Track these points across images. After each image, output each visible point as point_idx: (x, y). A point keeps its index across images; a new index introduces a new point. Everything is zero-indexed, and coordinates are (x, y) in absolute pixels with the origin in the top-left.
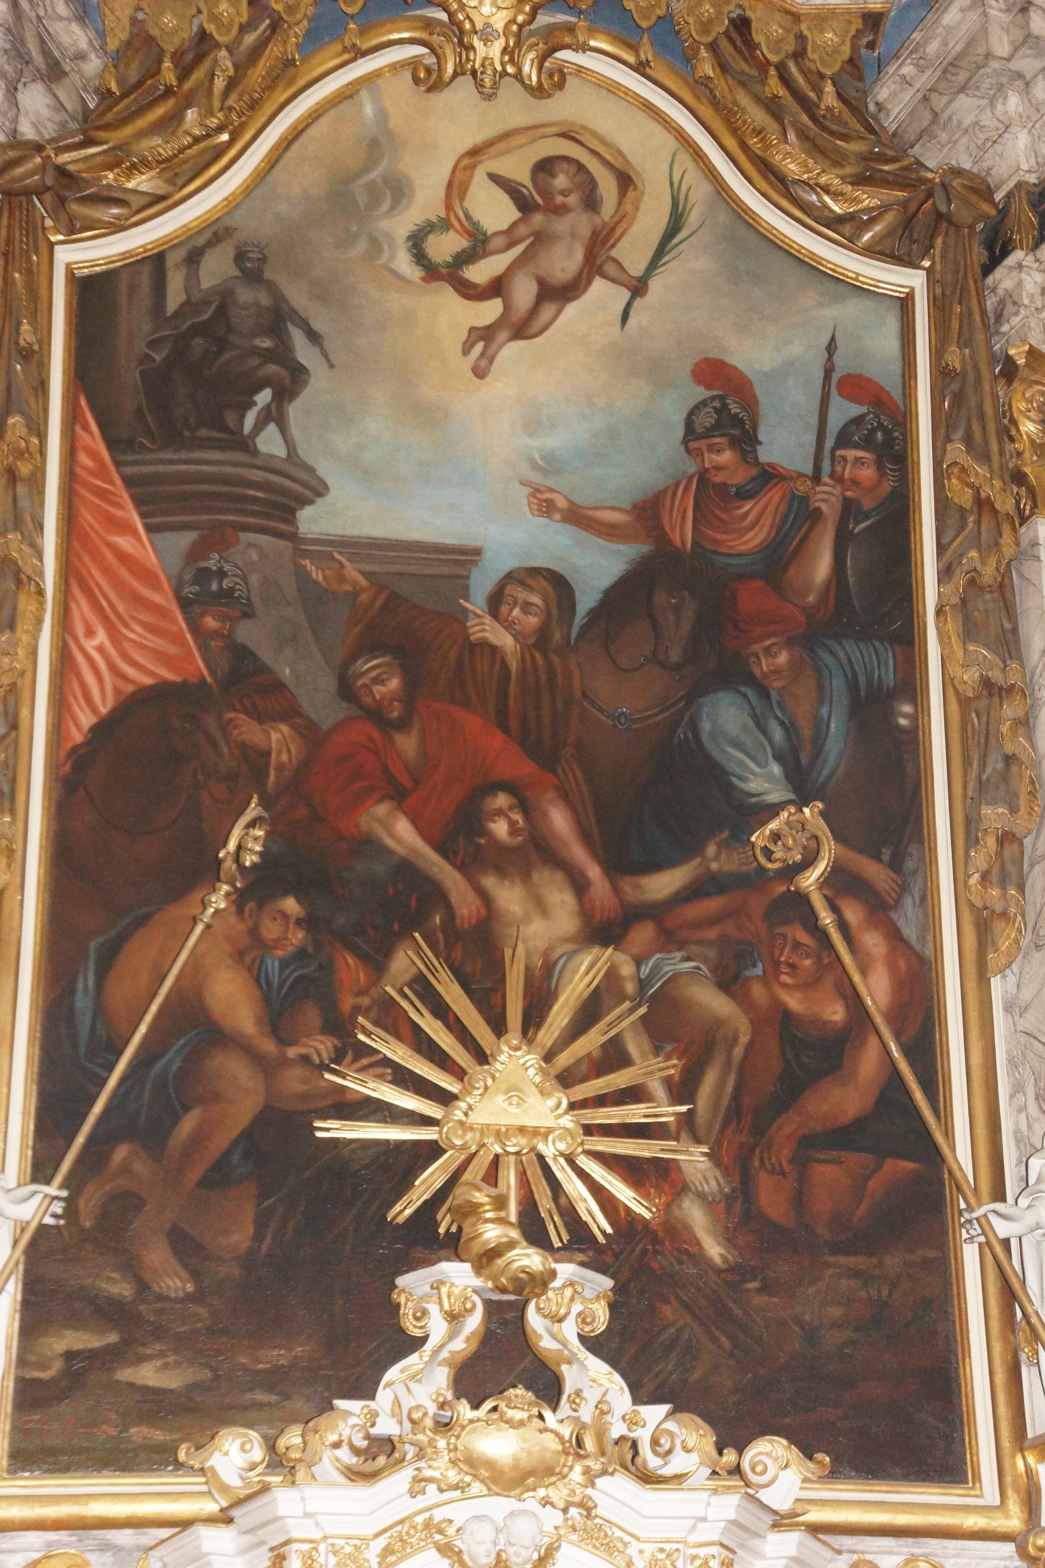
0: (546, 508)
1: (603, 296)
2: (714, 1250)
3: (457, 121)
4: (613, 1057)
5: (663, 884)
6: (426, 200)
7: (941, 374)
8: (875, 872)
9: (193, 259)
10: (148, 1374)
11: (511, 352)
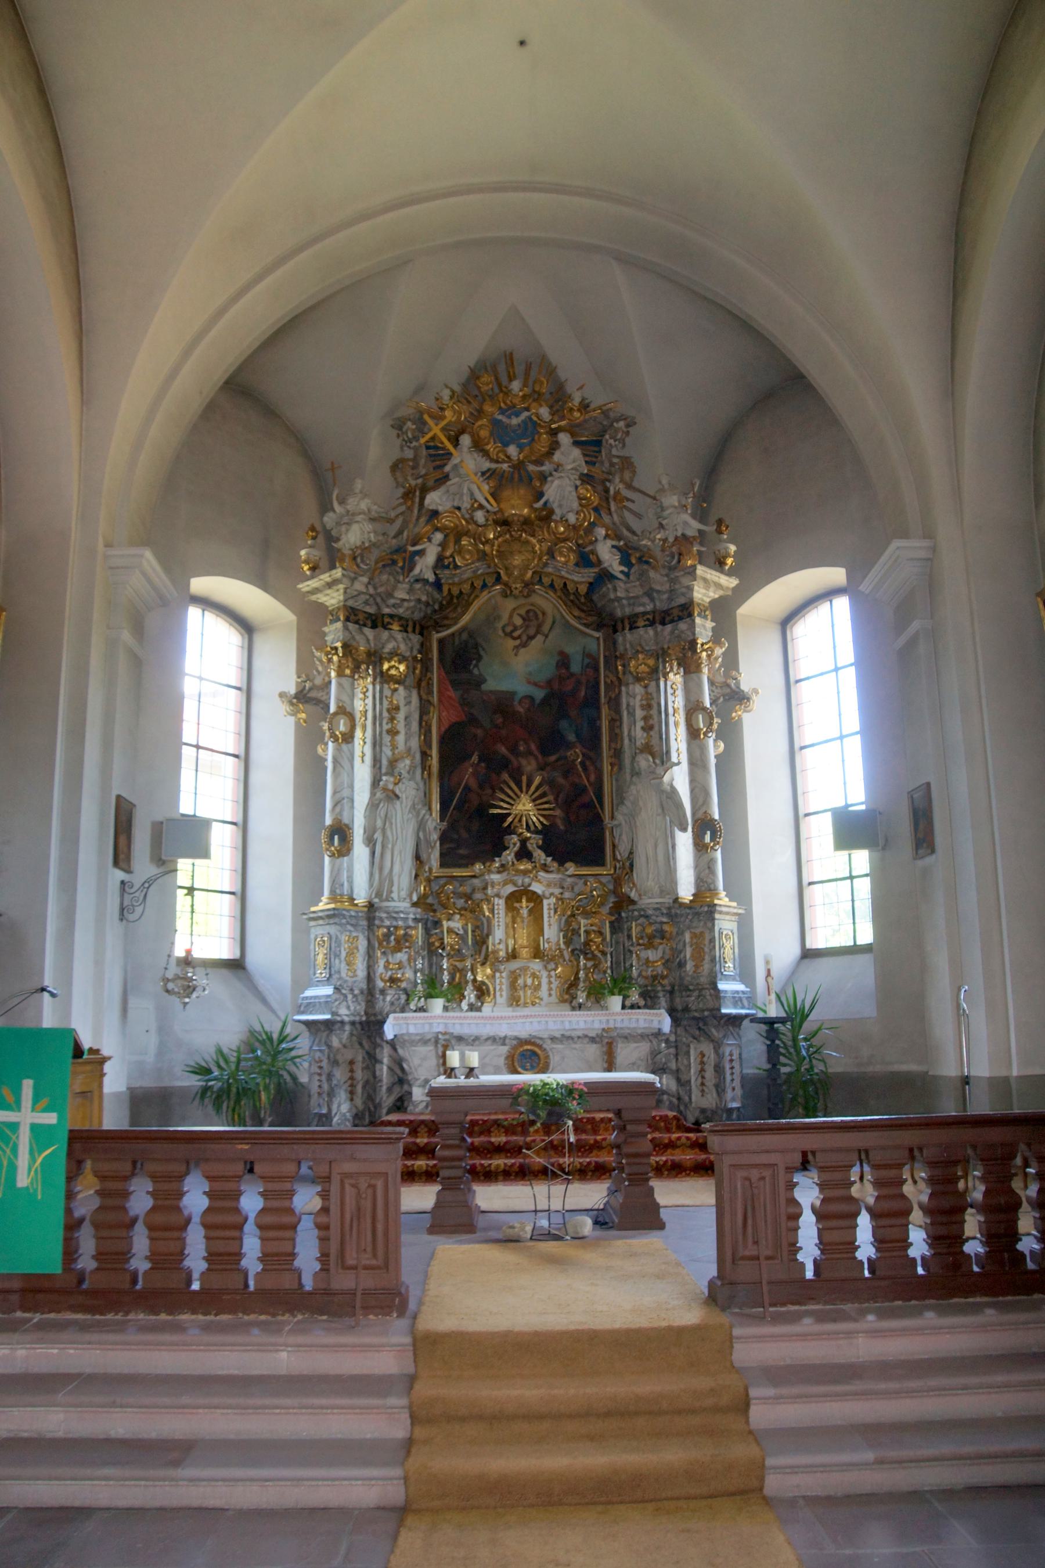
0: (529, 682)
1: (540, 638)
2: (562, 827)
4: (544, 795)
5: (553, 758)
6: (505, 619)
7: (605, 657)
8: (592, 754)
9: (460, 634)
10: (461, 851)
11: (522, 651)
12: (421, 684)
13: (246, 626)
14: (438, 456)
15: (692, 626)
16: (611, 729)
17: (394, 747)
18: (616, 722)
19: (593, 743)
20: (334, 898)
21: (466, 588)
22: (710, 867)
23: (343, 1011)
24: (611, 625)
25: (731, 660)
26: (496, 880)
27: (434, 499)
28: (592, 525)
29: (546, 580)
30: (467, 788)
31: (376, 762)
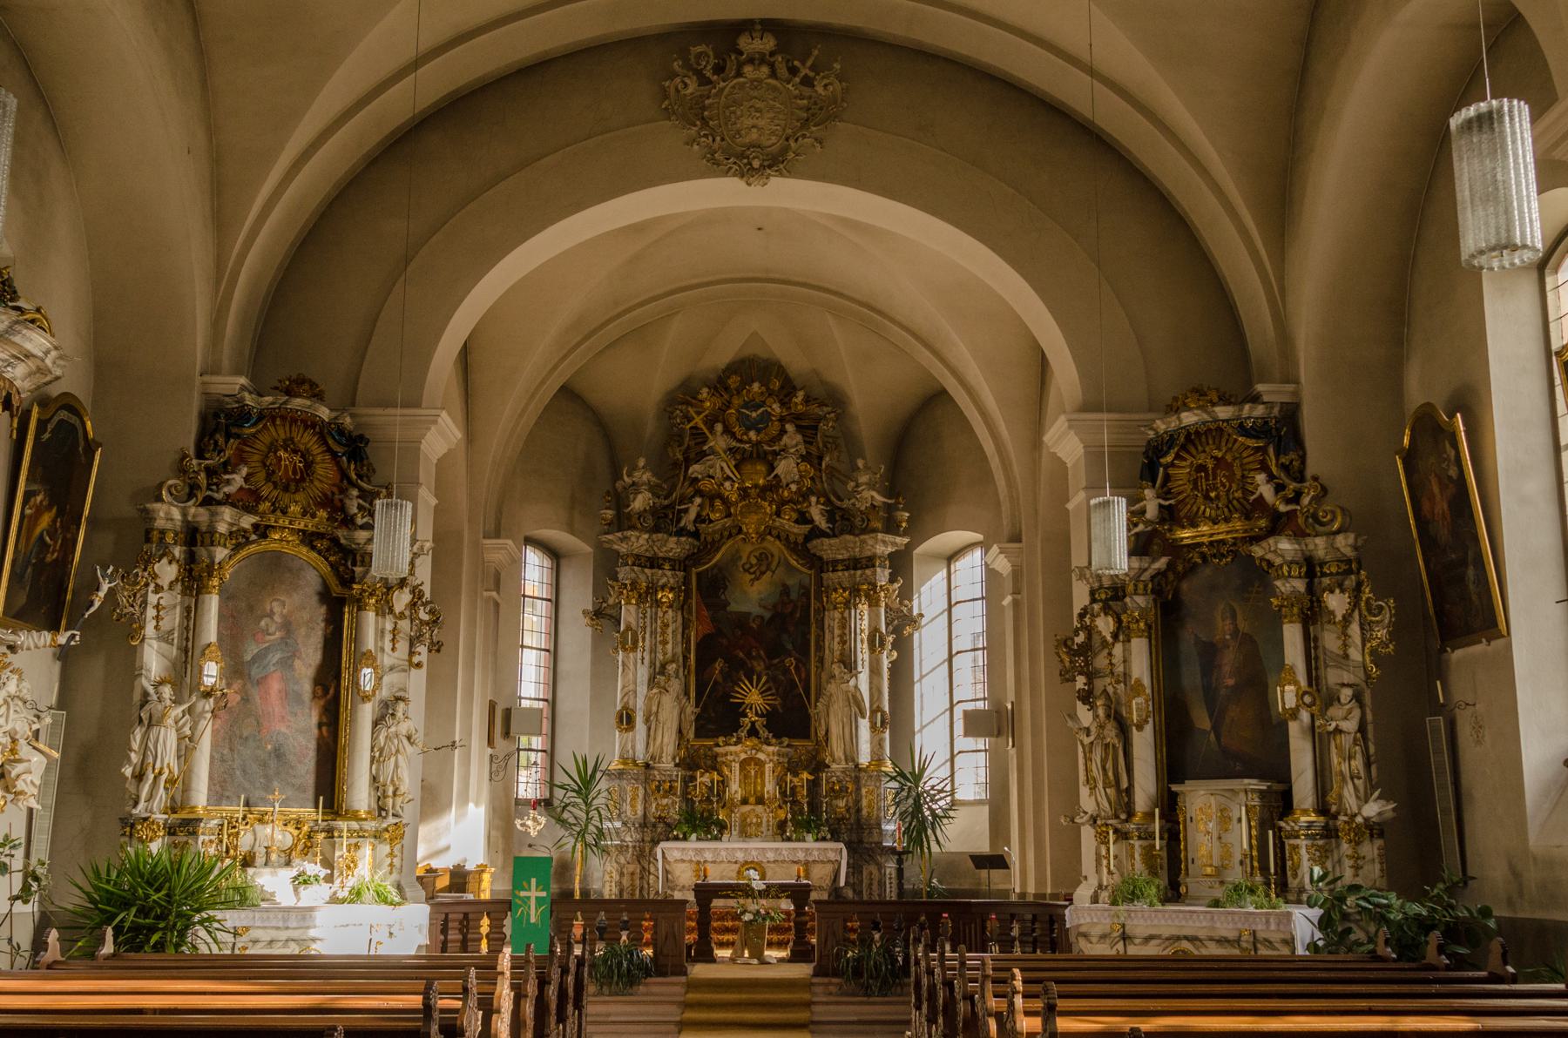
1: (769, 573)
3: (748, 548)
4: (769, 689)
6: (744, 560)
12: (683, 607)
13: (555, 554)
14: (699, 436)
15: (874, 573)
16: (817, 643)
17: (665, 654)
18: (820, 639)
19: (803, 650)
20: (624, 760)
21: (717, 537)
22: (880, 744)
23: (628, 839)
24: (819, 565)
25: (906, 593)
26: (734, 752)
27: (696, 469)
28: (810, 491)
29: (774, 532)
30: (716, 682)
31: (653, 664)
